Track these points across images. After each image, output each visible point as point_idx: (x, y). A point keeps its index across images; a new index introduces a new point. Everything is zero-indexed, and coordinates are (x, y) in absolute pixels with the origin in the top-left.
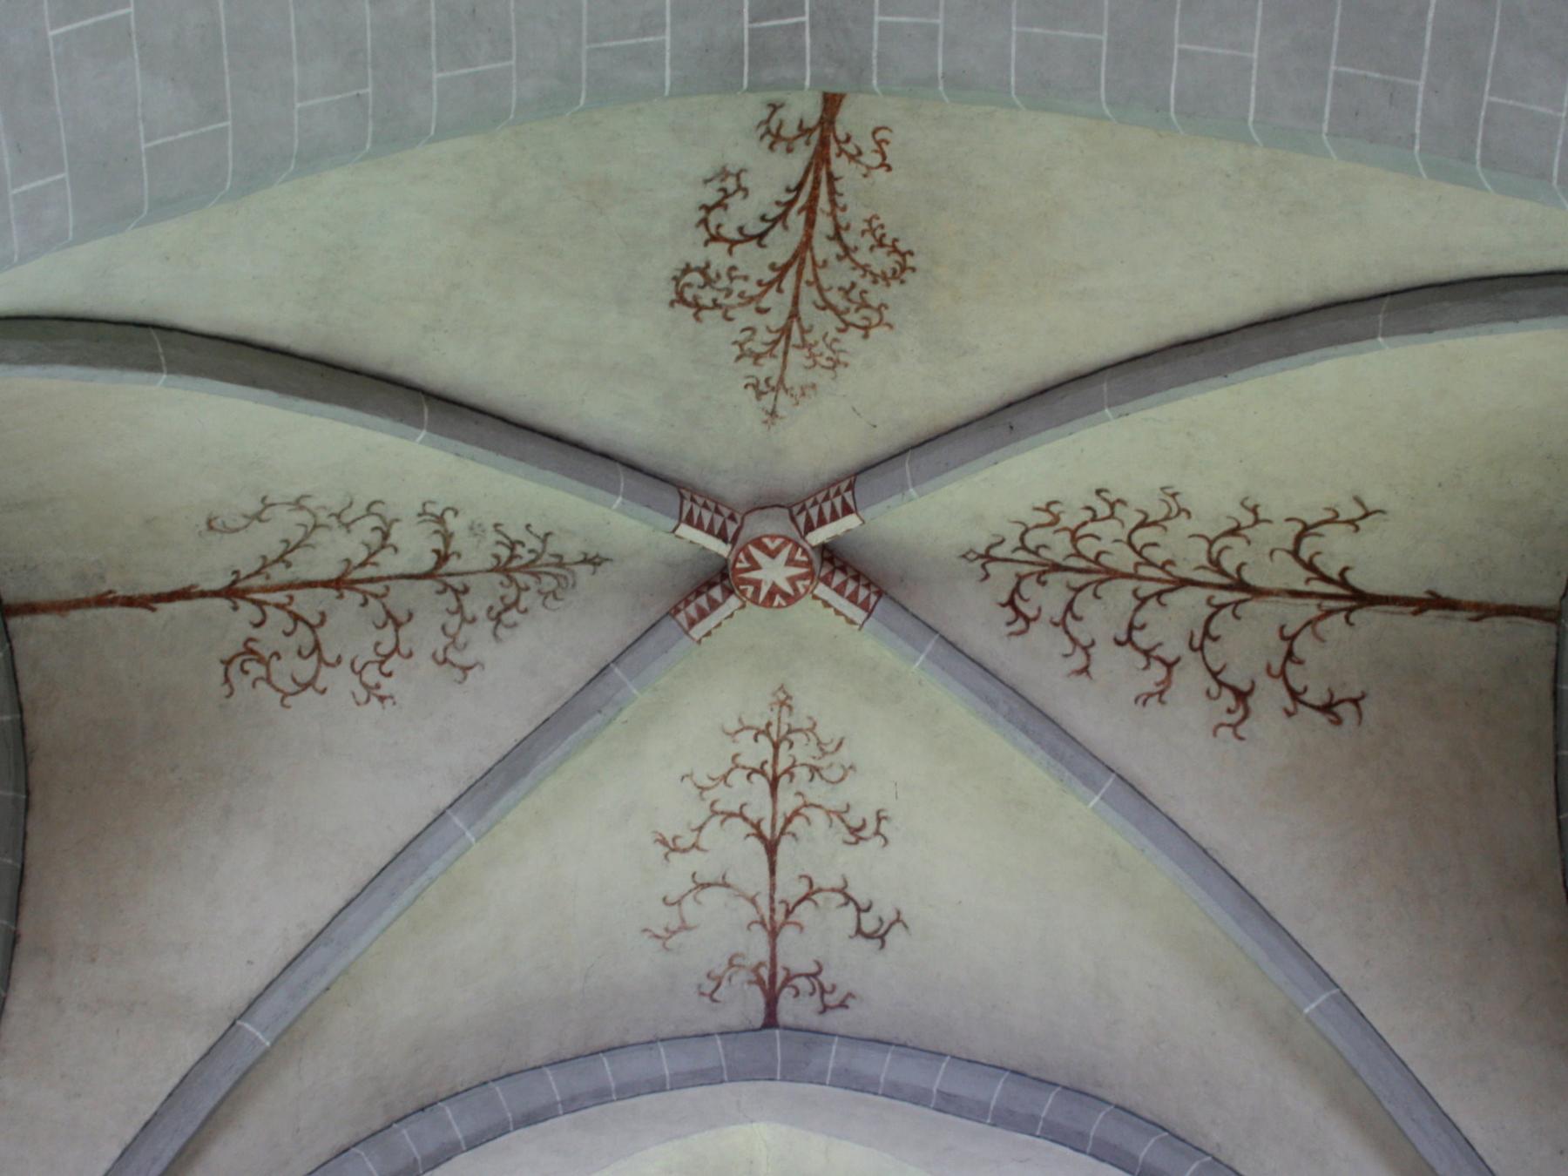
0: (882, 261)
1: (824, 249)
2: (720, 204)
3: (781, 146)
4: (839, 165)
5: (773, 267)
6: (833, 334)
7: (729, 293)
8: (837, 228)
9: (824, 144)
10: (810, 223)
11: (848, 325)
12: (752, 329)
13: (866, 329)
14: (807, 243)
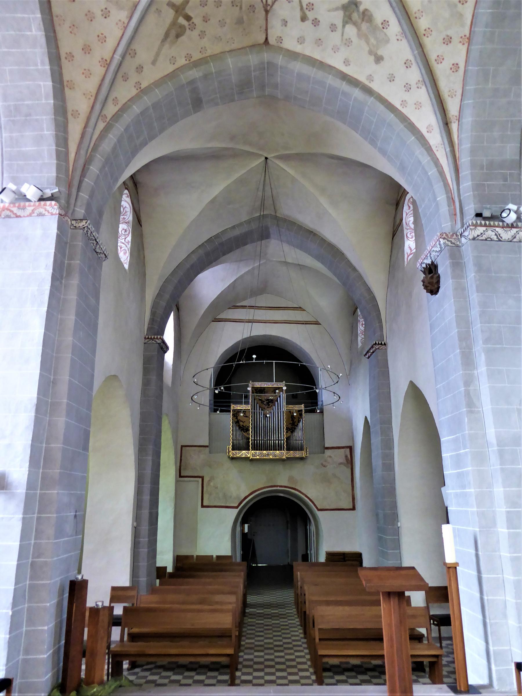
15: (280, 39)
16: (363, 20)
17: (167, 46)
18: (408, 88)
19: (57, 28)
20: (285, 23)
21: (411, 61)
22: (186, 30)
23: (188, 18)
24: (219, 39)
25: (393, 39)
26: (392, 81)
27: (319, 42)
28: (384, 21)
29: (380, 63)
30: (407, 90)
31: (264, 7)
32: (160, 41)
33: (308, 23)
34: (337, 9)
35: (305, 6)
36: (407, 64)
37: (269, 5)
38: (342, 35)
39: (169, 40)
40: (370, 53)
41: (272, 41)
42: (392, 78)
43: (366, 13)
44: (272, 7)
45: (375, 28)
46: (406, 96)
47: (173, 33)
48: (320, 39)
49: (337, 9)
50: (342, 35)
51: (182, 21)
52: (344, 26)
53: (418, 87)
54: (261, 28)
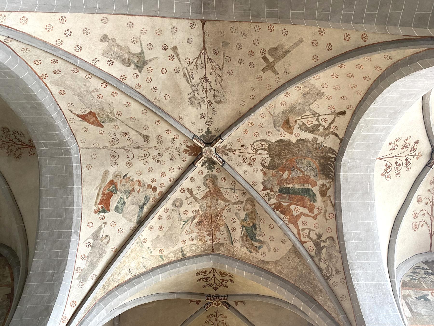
0: (17, 155)
1: (17, 146)
2: (19, 134)
3: (29, 141)
4: (29, 149)
5: (12, 140)
6: (6, 147)
7: (7, 134)
8: (20, 148)
9: (31, 147)
10: (20, 145)
11: (7, 150)
12: (2, 137)
13: (7, 152)
14: (17, 144)
15: (192, 26)
16: (128, 59)
17: (287, 47)
18: (68, 33)
19: (364, 92)
20: (189, 41)
21: (77, 52)
22: (269, 51)
23: (265, 58)
24: (243, 34)
25: (100, 57)
26: (85, 30)
27: (159, 33)
28: (112, 65)
29: (102, 37)
30: (67, 31)
31: (207, 52)
32: (291, 52)
33: (171, 46)
34: (151, 60)
35: (175, 57)
36: (79, 48)
37: (203, 54)
38: (141, 44)
39: (284, 50)
40: (113, 40)
41: (199, 24)
42: (86, 31)
43: (128, 64)
44: (201, 53)
45: (117, 58)
46: (65, 27)
47: (279, 53)
48: (159, 35)
49: (151, 60)
50: (141, 44)
51: (271, 59)
52: (142, 50)
53: (59, 40)
54: (209, 35)
